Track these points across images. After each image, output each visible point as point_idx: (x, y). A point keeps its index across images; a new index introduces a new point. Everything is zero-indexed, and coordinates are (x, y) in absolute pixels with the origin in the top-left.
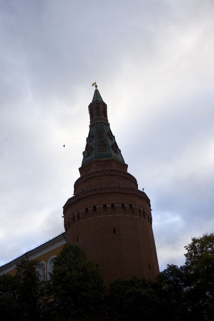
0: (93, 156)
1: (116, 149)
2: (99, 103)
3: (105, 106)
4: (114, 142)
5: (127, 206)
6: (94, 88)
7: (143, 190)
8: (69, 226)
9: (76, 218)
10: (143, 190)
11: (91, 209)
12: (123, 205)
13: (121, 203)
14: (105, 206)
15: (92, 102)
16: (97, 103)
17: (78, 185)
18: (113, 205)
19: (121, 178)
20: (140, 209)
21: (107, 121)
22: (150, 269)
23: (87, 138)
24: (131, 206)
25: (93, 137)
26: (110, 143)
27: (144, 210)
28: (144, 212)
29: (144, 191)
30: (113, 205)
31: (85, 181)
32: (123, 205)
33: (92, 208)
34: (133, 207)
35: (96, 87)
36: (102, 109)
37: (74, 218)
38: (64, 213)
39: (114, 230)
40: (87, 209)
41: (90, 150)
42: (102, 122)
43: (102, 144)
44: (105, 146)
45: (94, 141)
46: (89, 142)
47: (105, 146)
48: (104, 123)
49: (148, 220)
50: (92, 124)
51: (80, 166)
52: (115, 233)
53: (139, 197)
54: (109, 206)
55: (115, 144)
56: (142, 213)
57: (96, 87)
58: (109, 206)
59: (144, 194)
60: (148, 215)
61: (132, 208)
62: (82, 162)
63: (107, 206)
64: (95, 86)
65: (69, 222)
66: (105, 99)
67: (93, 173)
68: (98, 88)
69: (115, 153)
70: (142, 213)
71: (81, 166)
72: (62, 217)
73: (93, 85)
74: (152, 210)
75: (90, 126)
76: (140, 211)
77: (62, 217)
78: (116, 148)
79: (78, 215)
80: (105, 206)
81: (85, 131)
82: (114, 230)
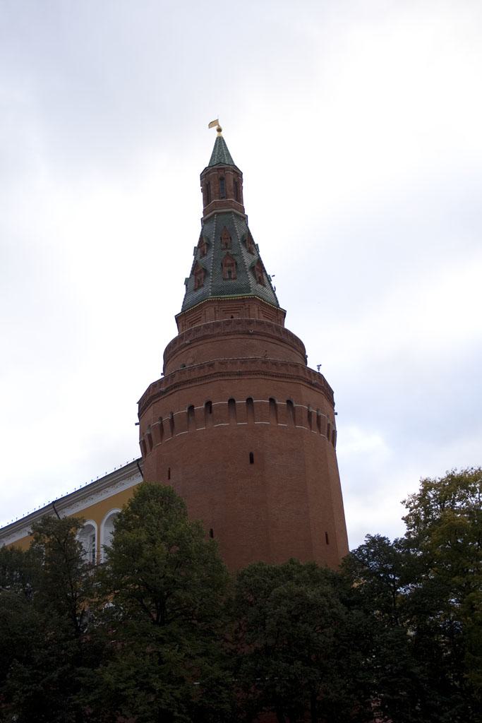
0: (207, 288)
1: (260, 275)
2: (224, 169)
3: (238, 175)
4: (256, 258)
5: (281, 403)
6: (216, 134)
7: (319, 369)
10: (319, 369)
12: (272, 400)
13: (269, 397)
14: (232, 401)
15: (209, 167)
16: (220, 169)
17: (171, 353)
18: (249, 400)
19: (270, 340)
20: (311, 410)
21: (243, 209)
22: (327, 543)
23: (195, 247)
24: (289, 402)
25: (209, 245)
26: (248, 260)
27: (320, 414)
28: (318, 417)
29: (322, 372)
30: (249, 400)
31: (189, 344)
32: (272, 400)
33: (204, 406)
34: (295, 405)
35: (219, 130)
36: (232, 184)
37: (161, 426)
38: (139, 415)
39: (251, 456)
40: (191, 408)
41: (203, 274)
42: (230, 212)
43: (229, 261)
44: (236, 267)
45: (211, 254)
46: (201, 258)
47: (236, 267)
48: (235, 214)
49: (328, 436)
50: (206, 217)
51: (179, 310)
52: (252, 461)
53: (308, 383)
54: (241, 402)
55: (259, 262)
56: (314, 419)
57: (219, 130)
58: (241, 402)
59: (320, 376)
60: (329, 425)
61: (293, 409)
62: (184, 302)
64: (216, 127)
65: (150, 436)
66: (239, 161)
67: (207, 327)
68: (223, 134)
69: (257, 283)
70: (314, 419)
71: (180, 311)
72: (136, 424)
73: (212, 124)
74: (336, 414)
75: (204, 221)
76: (310, 414)
77: (136, 424)
78: (261, 272)
79: (172, 421)
80: (232, 401)
81: (192, 232)
82: (251, 456)
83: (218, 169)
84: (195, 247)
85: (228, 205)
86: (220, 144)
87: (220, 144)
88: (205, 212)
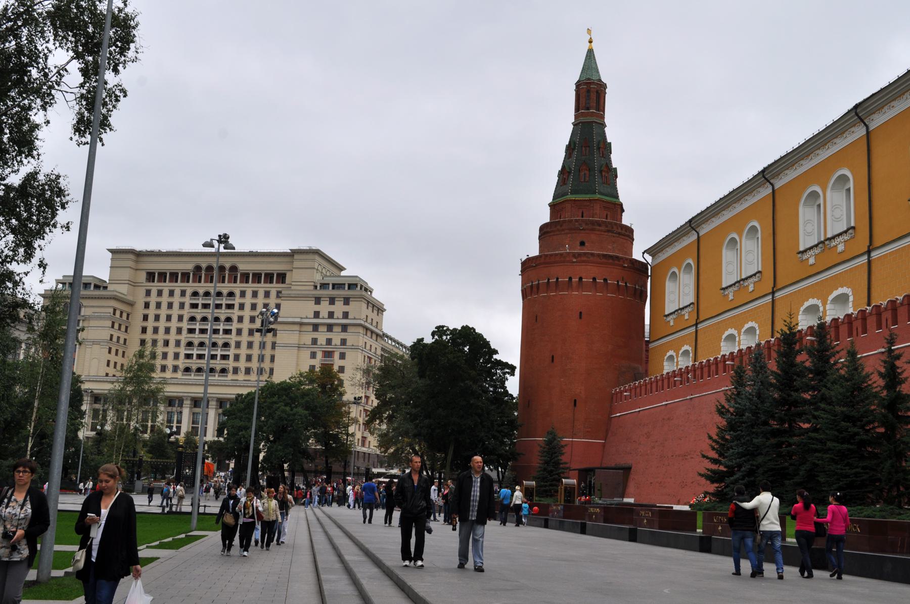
8: (526, 297)
9: (535, 289)
12: (594, 279)
14: (570, 279)
17: (545, 231)
18: (581, 279)
21: (603, 117)
25: (574, 149)
26: (597, 163)
32: (594, 279)
42: (593, 122)
46: (568, 159)
54: (575, 280)
58: (575, 280)
75: (575, 125)
80: (570, 279)
85: (592, 114)
86: (590, 54)
87: (590, 54)
88: (576, 117)
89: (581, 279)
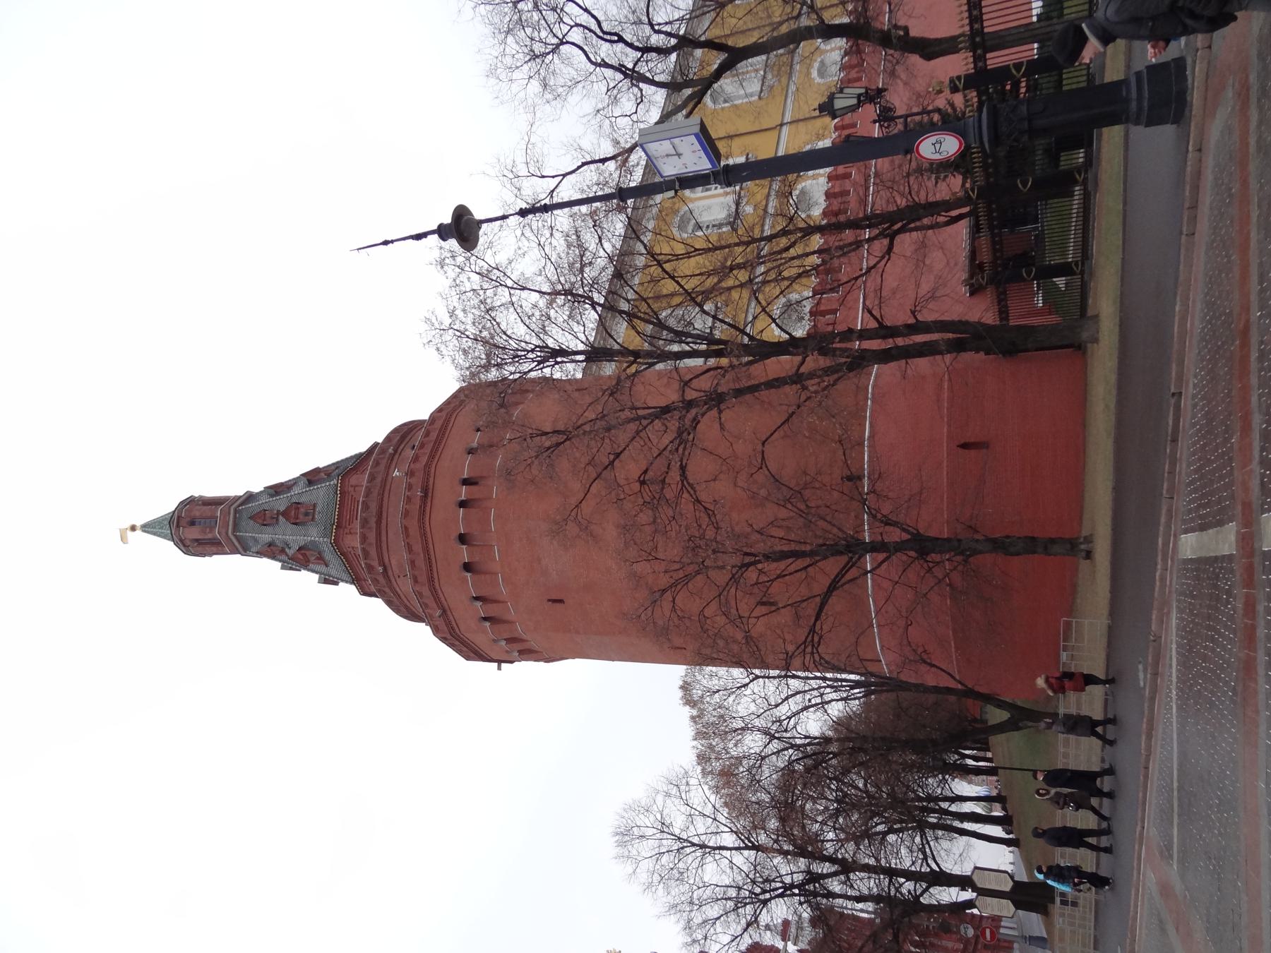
2: (179, 517)
3: (190, 502)
6: (139, 532)
9: (493, 610)
11: (465, 554)
14: (463, 504)
16: (178, 522)
18: (465, 482)
35: (133, 528)
50: (240, 549)
54: (464, 493)
57: (133, 528)
58: (464, 493)
63: (463, 498)
64: (130, 533)
71: (353, 587)
72: (499, 668)
77: (499, 668)
80: (463, 504)
83: (178, 526)
84: (283, 568)
86: (149, 528)
87: (149, 528)
88: (234, 551)
89: (465, 482)
